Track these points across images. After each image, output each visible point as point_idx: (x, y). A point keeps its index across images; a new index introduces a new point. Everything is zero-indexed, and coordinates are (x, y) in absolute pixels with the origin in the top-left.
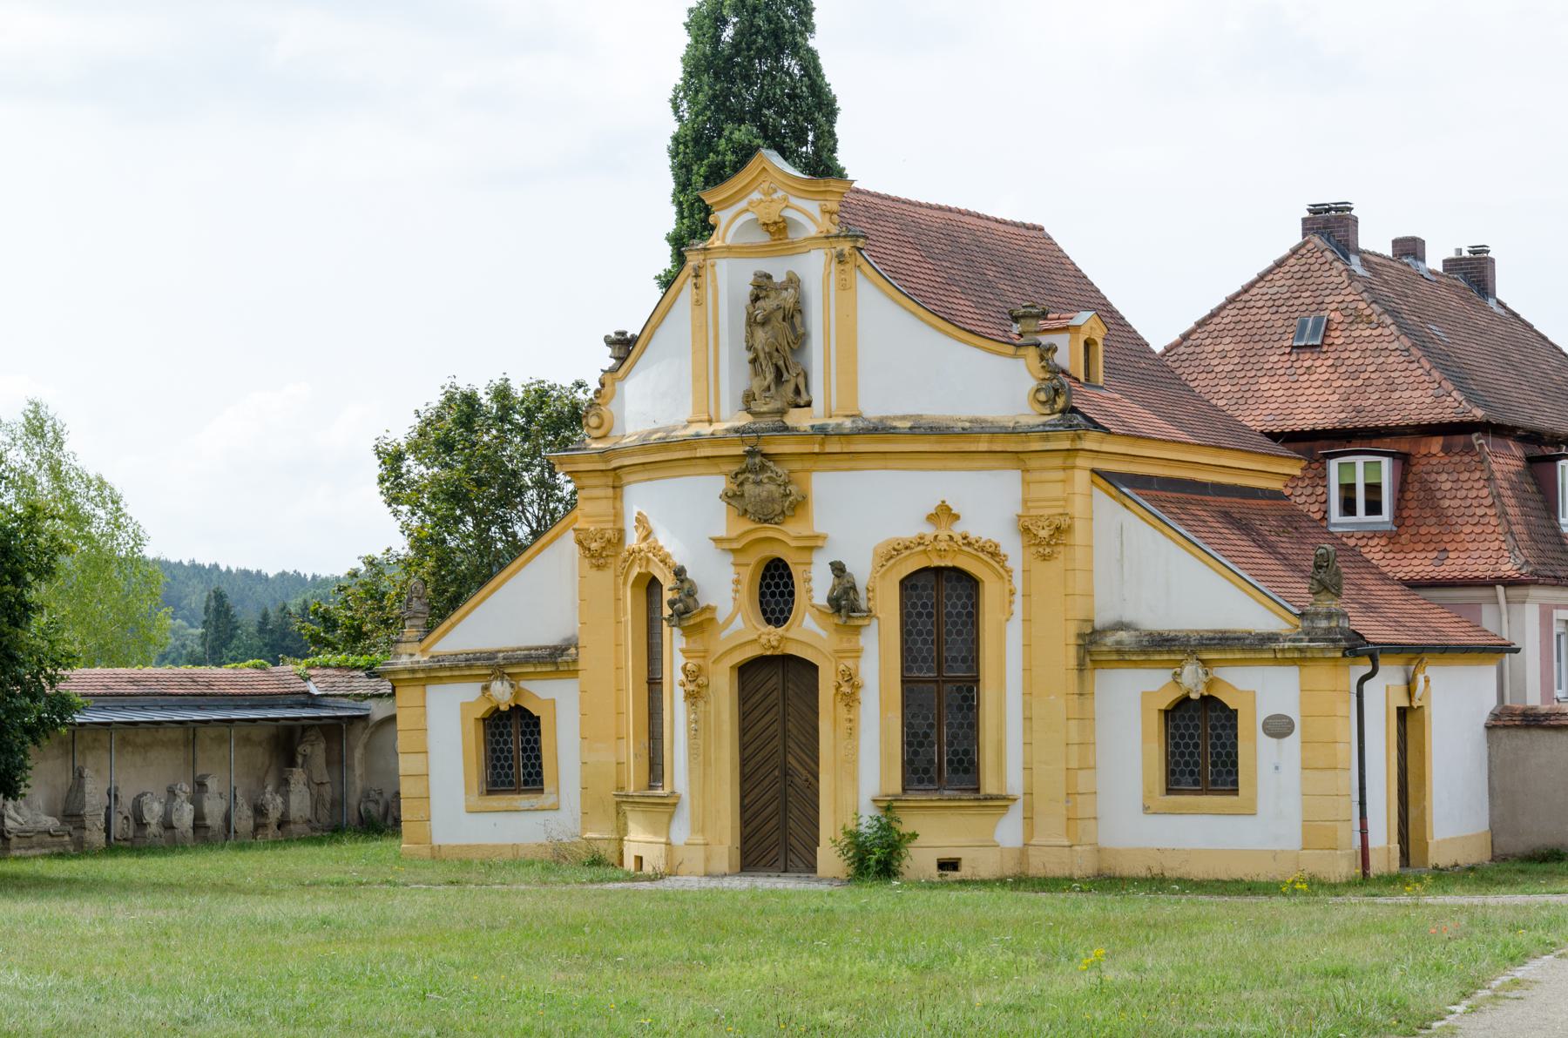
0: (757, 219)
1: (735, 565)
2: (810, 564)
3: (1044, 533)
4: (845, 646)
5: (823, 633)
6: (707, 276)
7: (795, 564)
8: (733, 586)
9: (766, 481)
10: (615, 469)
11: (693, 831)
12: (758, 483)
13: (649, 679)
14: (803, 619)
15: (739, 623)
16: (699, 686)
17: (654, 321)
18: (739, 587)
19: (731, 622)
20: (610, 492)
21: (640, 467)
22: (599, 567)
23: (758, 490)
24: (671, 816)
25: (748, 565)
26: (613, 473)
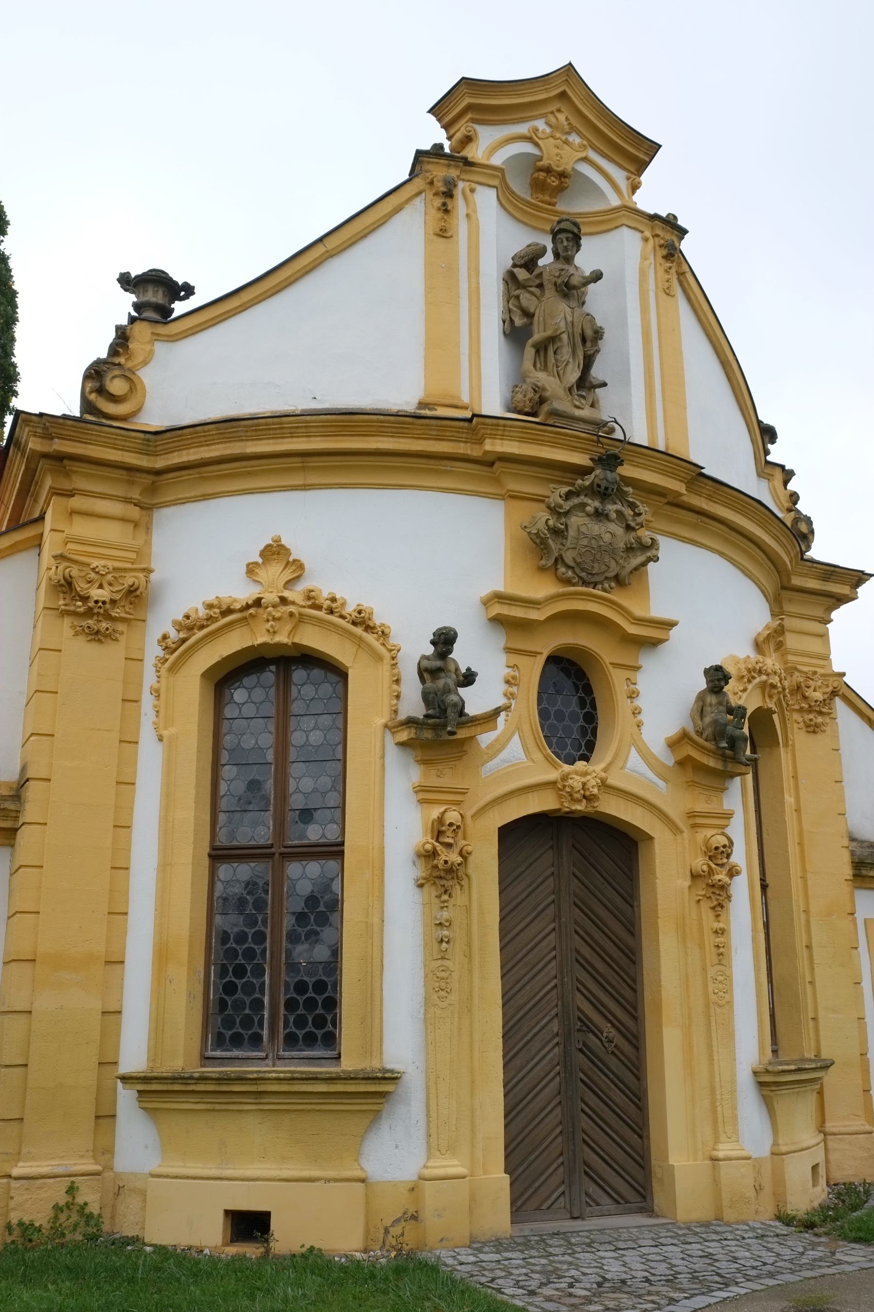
0: (541, 159)
1: (509, 650)
2: (637, 668)
3: (818, 696)
4: (701, 806)
5: (661, 783)
6: (460, 206)
7: (615, 665)
8: (503, 687)
9: (613, 516)
10: (158, 473)
11: (432, 1148)
12: (599, 515)
13: (213, 848)
14: (628, 756)
15: (514, 750)
16: (461, 854)
17: (331, 243)
18: (514, 689)
19: (499, 751)
20: (134, 512)
21: (296, 462)
22: (96, 636)
23: (595, 527)
24: (376, 1116)
25: (534, 654)
26: (148, 480)
